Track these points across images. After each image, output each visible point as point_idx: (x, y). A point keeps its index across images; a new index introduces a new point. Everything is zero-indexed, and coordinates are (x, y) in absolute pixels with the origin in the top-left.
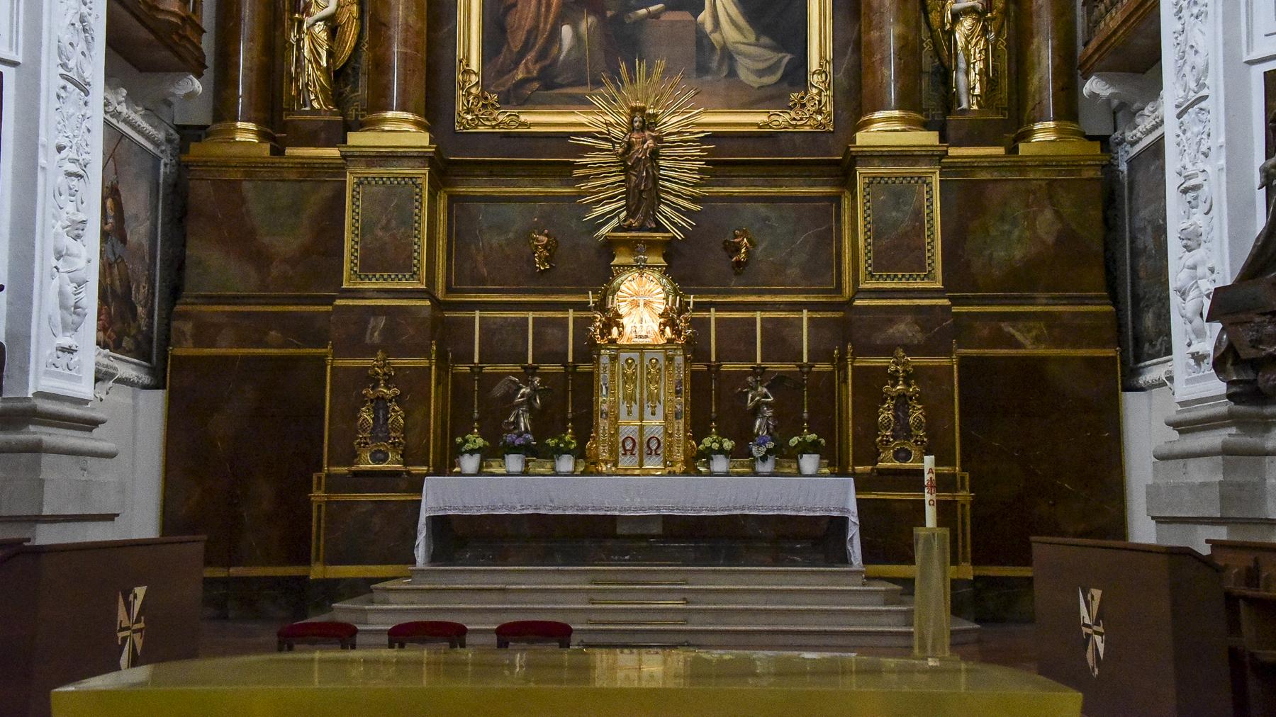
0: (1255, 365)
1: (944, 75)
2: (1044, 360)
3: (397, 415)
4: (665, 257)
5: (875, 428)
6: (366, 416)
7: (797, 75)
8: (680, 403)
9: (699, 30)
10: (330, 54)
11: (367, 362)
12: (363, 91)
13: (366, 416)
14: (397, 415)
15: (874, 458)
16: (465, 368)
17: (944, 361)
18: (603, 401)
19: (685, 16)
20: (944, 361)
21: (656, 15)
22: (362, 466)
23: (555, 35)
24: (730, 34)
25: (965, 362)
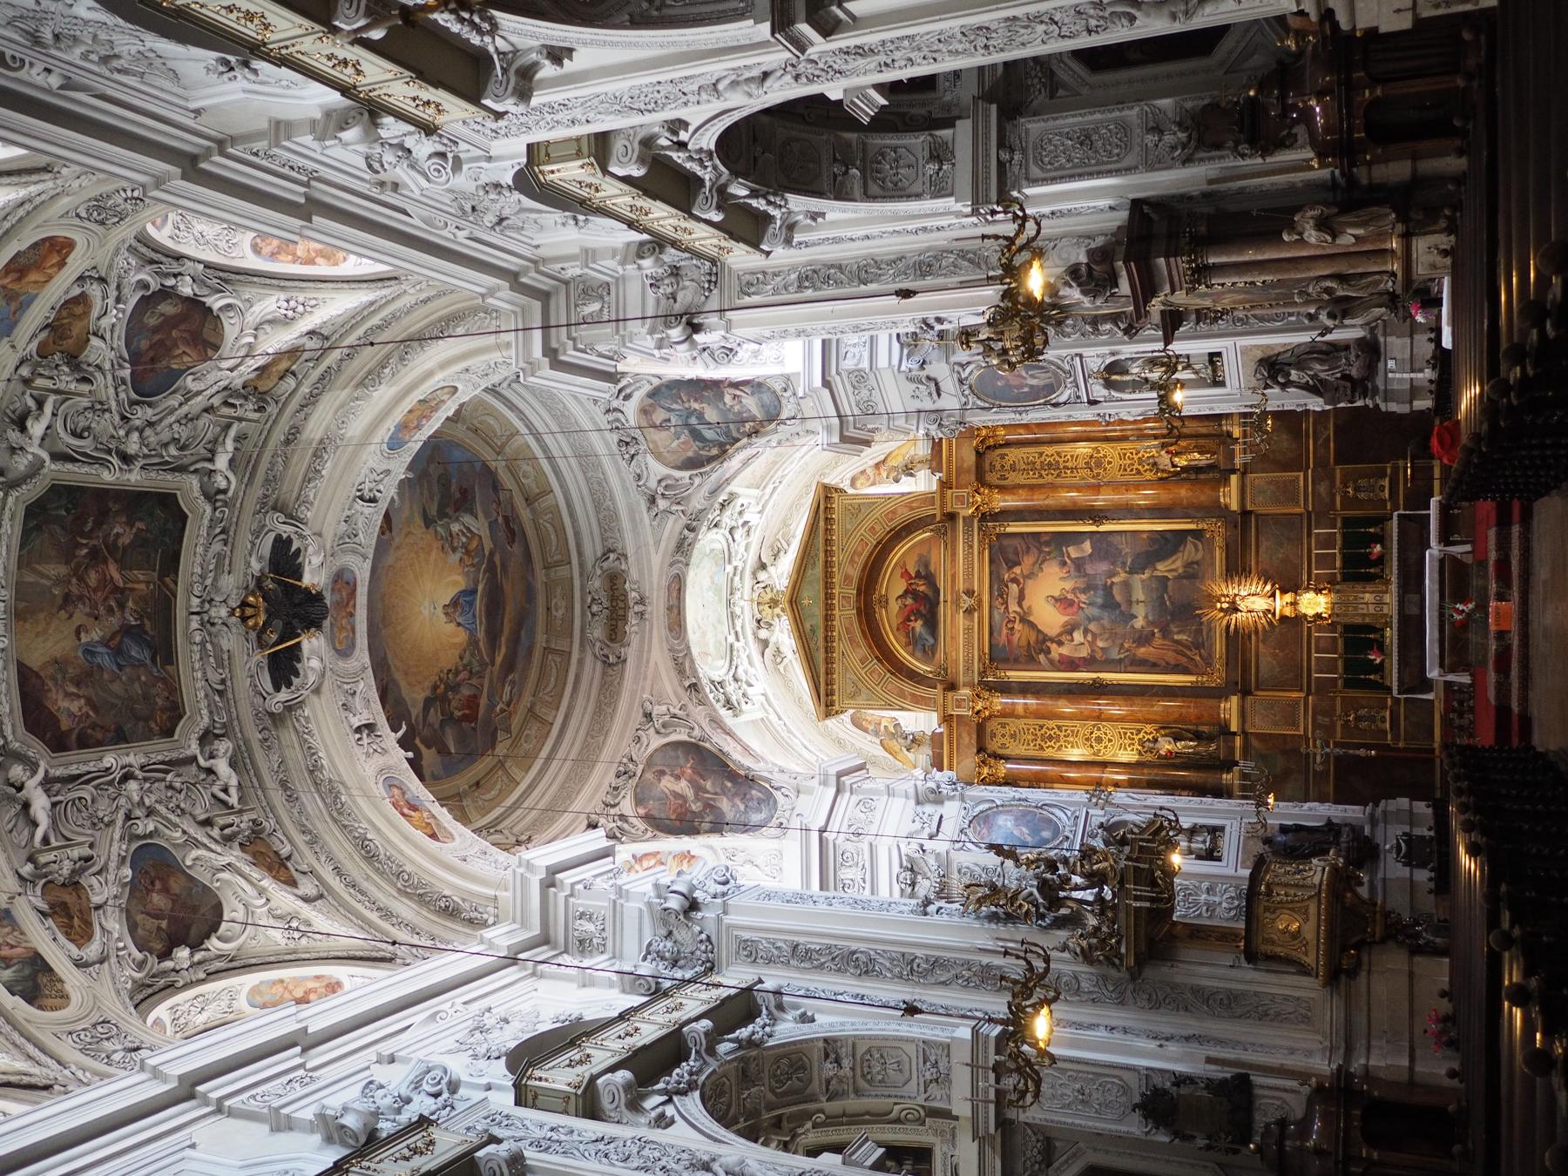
0: (1353, 392)
1: (1198, 470)
2: (1336, 426)
3: (1362, 712)
4: (1286, 592)
5: (1370, 500)
6: (1363, 725)
7: (1197, 534)
8: (1359, 587)
9: (1175, 578)
10: (1191, 740)
11: (1339, 723)
12: (1205, 729)
13: (1363, 725)
14: (1362, 712)
15: (1384, 501)
16: (1340, 682)
17: (1338, 471)
18: (1358, 620)
19: (1170, 583)
20: (1338, 471)
21: (1170, 598)
22: (1388, 726)
23: (1178, 642)
24: (1179, 564)
25: (1337, 462)
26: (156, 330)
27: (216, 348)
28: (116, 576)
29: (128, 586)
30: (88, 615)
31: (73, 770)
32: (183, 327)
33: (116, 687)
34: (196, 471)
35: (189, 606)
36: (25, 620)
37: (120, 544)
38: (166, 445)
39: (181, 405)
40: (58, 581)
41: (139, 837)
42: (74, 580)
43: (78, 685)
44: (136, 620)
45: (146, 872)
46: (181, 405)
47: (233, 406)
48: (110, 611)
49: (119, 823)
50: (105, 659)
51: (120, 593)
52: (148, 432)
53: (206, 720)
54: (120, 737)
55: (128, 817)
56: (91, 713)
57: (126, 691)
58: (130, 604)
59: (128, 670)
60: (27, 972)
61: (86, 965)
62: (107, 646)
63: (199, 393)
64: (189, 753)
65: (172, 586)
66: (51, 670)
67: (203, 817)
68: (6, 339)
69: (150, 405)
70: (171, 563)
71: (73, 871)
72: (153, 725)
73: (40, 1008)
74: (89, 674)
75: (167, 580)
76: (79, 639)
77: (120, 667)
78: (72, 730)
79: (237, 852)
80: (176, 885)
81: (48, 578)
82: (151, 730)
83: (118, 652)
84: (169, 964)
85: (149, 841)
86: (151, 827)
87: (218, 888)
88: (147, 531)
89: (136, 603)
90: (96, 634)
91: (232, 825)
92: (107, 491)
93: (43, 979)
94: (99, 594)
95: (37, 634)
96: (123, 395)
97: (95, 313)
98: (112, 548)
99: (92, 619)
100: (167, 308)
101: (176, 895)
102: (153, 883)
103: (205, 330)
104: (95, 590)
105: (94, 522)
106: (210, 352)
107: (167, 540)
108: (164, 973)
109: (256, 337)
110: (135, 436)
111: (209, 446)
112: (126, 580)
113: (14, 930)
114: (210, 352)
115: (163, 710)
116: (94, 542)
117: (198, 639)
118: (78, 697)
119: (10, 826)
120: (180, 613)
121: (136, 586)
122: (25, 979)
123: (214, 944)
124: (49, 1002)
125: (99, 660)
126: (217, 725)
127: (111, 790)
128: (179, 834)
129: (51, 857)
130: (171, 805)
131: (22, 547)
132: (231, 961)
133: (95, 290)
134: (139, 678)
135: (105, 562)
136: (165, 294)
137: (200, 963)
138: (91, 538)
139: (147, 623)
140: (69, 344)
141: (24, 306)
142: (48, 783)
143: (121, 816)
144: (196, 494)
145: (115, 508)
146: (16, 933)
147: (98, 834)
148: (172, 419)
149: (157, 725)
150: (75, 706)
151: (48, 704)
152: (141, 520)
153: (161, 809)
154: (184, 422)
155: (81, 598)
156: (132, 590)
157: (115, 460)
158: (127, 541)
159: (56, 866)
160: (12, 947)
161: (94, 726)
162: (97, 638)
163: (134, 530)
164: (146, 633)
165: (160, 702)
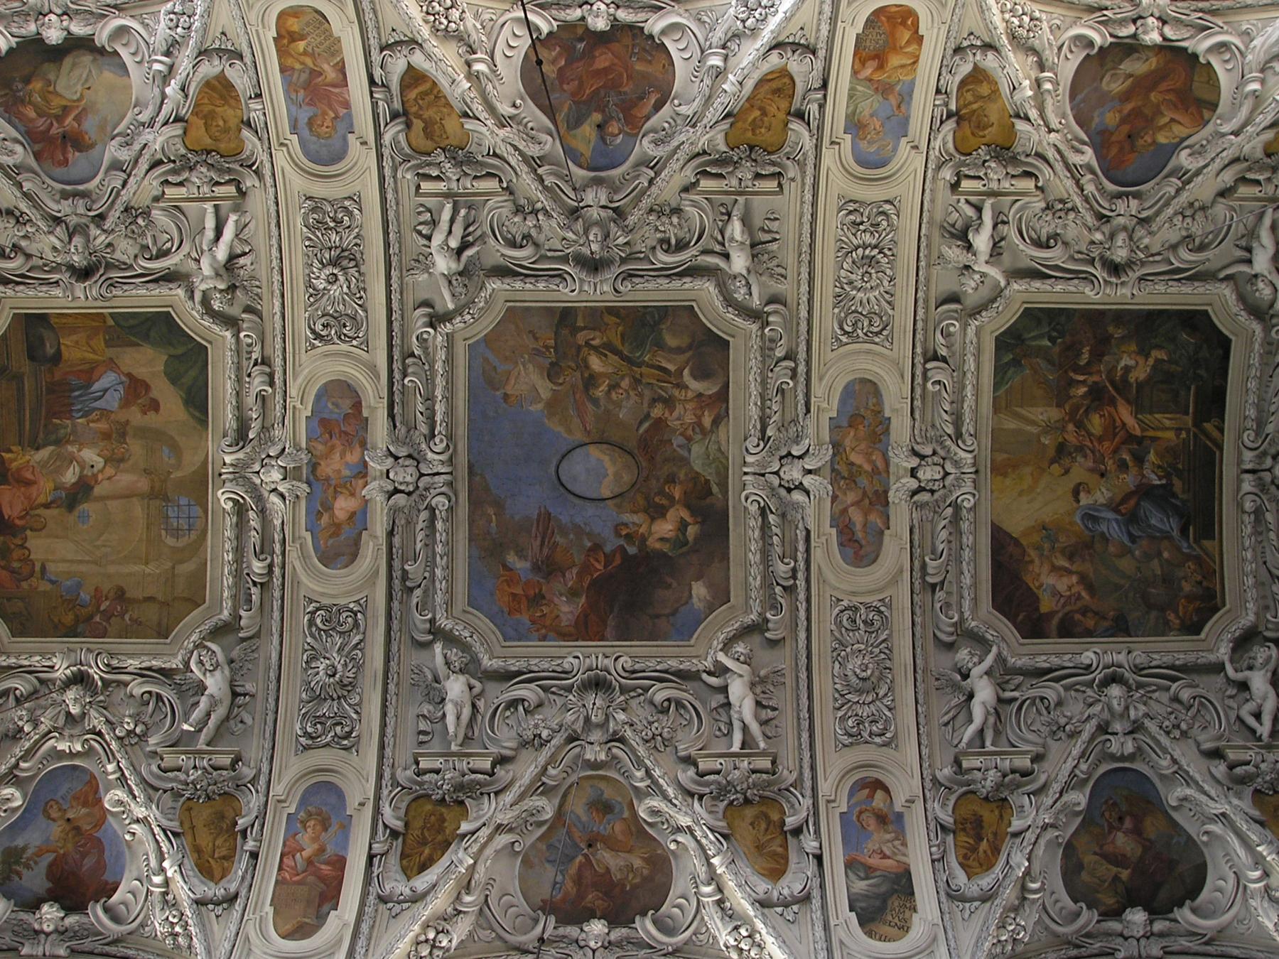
26: (1126, 96)
27: (1214, 106)
28: (1130, 421)
29: (1151, 433)
30: (1092, 470)
31: (1042, 662)
32: (1163, 86)
33: (1125, 564)
34: (1228, 278)
35: (1240, 461)
36: (1005, 475)
37: (1132, 380)
38: (1174, 247)
39: (1178, 191)
40: (1048, 429)
41: (1113, 758)
42: (1071, 427)
43: (1071, 558)
44: (1160, 478)
45: (1115, 804)
46: (1178, 191)
47: (1258, 182)
48: (1123, 466)
49: (1085, 736)
50: (1112, 527)
51: (1138, 445)
52: (1140, 232)
53: (1252, 617)
54: (1121, 627)
55: (1103, 729)
56: (1084, 594)
57: (1138, 569)
58: (1152, 457)
59: (1144, 543)
60: (883, 889)
61: (964, 899)
62: (1116, 510)
63: (1198, 172)
64: (1212, 658)
65: (1215, 434)
66: (1036, 538)
67: (1207, 746)
68: (904, 140)
69: (1137, 196)
70: (1213, 403)
71: (999, 786)
72: (1171, 617)
73: (870, 934)
74: (1089, 545)
75: (1207, 426)
76: (1078, 501)
77: (1133, 539)
78: (1051, 614)
79: (1246, 804)
80: (1152, 828)
81: (1033, 423)
82: (1167, 623)
83: (1132, 519)
84: (1114, 926)
85: (1127, 765)
86: (1129, 748)
87: (1206, 844)
88: (1170, 362)
89: (1157, 454)
90: (1101, 495)
91: (1248, 763)
92: (1102, 313)
93: (895, 902)
94: (1106, 444)
95: (1021, 494)
96: (1090, 188)
97: (1005, 89)
98: (1122, 386)
99: (1097, 477)
100: (1136, 67)
101: (1149, 840)
102: (1121, 819)
103: (1195, 85)
104: (1100, 440)
105: (1091, 352)
106: (1206, 114)
107: (1202, 372)
108: (1109, 934)
109: (1263, 82)
110: (1121, 239)
111: (1243, 243)
112: (1144, 426)
113: (897, 838)
114: (1206, 114)
115: (1190, 598)
116: (1095, 378)
117: (1248, 506)
118: (1069, 572)
119: (946, 718)
120: (1229, 471)
121: (1159, 434)
122: (877, 896)
123: (1185, 915)
124: (886, 929)
125: (1103, 527)
126: (1270, 626)
127: (1089, 692)
128: (1164, 763)
129: (975, 762)
130: (1167, 723)
131: (997, 386)
132: (1206, 943)
133: (797, 65)
134: (1159, 554)
135: (1113, 402)
136: (1128, 48)
137: (1161, 935)
138: (1090, 374)
139: (1176, 481)
140: (991, 133)
141: (906, 97)
142: (1002, 674)
143: (1090, 728)
144: (1235, 310)
145: (1118, 333)
146: (897, 843)
147: (1054, 746)
148: (1170, 211)
149: (1178, 617)
150: (1062, 584)
151: (1028, 579)
152: (1159, 347)
153: (1151, 726)
154: (1188, 213)
155: (1080, 449)
156: (1154, 439)
157: (1100, 273)
158: (1142, 376)
159: (978, 775)
160: (885, 857)
161: (1085, 611)
162: (1102, 500)
163: (1151, 361)
164: (1174, 495)
165: (1187, 587)
